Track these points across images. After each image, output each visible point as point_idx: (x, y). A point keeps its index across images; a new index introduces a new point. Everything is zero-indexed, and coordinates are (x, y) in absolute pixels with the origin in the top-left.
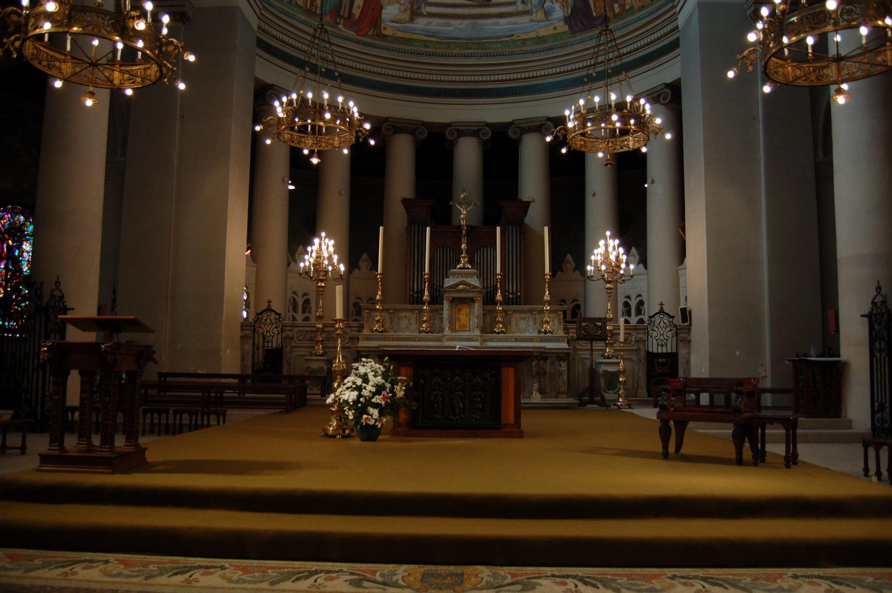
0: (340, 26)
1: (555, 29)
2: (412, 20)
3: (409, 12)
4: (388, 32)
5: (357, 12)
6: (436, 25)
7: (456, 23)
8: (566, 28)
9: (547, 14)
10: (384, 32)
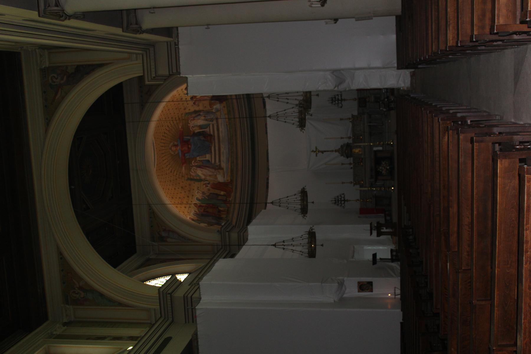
0: (230, 199)
1: (224, 107)
2: (222, 169)
3: (219, 170)
4: (229, 179)
5: (222, 193)
6: (224, 158)
7: (222, 150)
8: (224, 103)
9: (218, 110)
10: (229, 181)
